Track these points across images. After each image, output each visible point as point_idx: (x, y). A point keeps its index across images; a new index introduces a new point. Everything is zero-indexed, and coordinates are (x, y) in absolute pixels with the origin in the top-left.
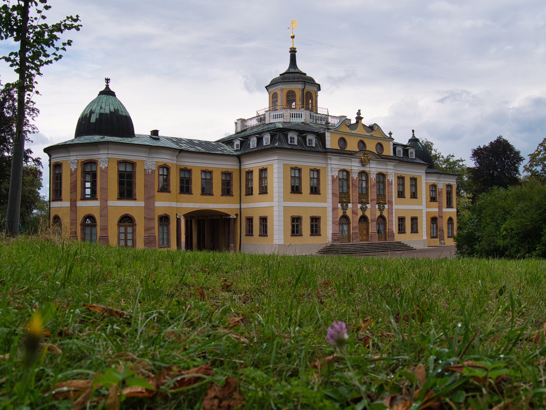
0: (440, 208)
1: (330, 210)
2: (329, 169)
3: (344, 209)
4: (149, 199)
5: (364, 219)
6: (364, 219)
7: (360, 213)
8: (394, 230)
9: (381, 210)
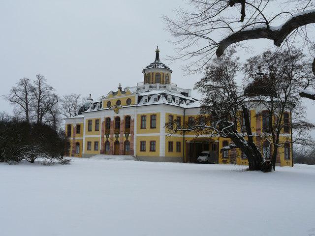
3: (107, 138)
4: (74, 137)
5: (117, 143)
6: (117, 143)
7: (115, 139)
8: (135, 149)
9: (127, 137)
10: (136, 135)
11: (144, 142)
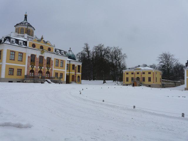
0: (76, 72)
1: (26, 68)
2: (27, 54)
5: (40, 72)
6: (40, 72)
10: (53, 69)
11: (57, 73)
